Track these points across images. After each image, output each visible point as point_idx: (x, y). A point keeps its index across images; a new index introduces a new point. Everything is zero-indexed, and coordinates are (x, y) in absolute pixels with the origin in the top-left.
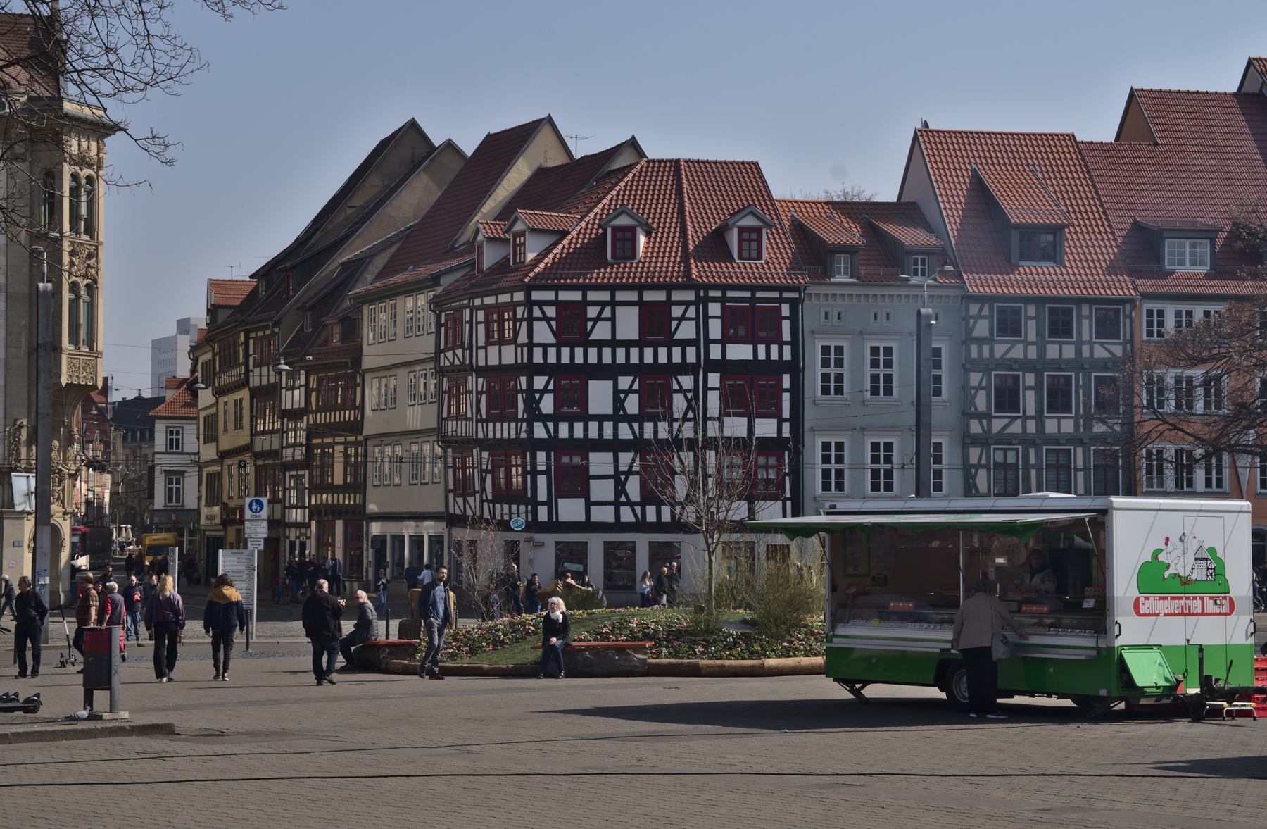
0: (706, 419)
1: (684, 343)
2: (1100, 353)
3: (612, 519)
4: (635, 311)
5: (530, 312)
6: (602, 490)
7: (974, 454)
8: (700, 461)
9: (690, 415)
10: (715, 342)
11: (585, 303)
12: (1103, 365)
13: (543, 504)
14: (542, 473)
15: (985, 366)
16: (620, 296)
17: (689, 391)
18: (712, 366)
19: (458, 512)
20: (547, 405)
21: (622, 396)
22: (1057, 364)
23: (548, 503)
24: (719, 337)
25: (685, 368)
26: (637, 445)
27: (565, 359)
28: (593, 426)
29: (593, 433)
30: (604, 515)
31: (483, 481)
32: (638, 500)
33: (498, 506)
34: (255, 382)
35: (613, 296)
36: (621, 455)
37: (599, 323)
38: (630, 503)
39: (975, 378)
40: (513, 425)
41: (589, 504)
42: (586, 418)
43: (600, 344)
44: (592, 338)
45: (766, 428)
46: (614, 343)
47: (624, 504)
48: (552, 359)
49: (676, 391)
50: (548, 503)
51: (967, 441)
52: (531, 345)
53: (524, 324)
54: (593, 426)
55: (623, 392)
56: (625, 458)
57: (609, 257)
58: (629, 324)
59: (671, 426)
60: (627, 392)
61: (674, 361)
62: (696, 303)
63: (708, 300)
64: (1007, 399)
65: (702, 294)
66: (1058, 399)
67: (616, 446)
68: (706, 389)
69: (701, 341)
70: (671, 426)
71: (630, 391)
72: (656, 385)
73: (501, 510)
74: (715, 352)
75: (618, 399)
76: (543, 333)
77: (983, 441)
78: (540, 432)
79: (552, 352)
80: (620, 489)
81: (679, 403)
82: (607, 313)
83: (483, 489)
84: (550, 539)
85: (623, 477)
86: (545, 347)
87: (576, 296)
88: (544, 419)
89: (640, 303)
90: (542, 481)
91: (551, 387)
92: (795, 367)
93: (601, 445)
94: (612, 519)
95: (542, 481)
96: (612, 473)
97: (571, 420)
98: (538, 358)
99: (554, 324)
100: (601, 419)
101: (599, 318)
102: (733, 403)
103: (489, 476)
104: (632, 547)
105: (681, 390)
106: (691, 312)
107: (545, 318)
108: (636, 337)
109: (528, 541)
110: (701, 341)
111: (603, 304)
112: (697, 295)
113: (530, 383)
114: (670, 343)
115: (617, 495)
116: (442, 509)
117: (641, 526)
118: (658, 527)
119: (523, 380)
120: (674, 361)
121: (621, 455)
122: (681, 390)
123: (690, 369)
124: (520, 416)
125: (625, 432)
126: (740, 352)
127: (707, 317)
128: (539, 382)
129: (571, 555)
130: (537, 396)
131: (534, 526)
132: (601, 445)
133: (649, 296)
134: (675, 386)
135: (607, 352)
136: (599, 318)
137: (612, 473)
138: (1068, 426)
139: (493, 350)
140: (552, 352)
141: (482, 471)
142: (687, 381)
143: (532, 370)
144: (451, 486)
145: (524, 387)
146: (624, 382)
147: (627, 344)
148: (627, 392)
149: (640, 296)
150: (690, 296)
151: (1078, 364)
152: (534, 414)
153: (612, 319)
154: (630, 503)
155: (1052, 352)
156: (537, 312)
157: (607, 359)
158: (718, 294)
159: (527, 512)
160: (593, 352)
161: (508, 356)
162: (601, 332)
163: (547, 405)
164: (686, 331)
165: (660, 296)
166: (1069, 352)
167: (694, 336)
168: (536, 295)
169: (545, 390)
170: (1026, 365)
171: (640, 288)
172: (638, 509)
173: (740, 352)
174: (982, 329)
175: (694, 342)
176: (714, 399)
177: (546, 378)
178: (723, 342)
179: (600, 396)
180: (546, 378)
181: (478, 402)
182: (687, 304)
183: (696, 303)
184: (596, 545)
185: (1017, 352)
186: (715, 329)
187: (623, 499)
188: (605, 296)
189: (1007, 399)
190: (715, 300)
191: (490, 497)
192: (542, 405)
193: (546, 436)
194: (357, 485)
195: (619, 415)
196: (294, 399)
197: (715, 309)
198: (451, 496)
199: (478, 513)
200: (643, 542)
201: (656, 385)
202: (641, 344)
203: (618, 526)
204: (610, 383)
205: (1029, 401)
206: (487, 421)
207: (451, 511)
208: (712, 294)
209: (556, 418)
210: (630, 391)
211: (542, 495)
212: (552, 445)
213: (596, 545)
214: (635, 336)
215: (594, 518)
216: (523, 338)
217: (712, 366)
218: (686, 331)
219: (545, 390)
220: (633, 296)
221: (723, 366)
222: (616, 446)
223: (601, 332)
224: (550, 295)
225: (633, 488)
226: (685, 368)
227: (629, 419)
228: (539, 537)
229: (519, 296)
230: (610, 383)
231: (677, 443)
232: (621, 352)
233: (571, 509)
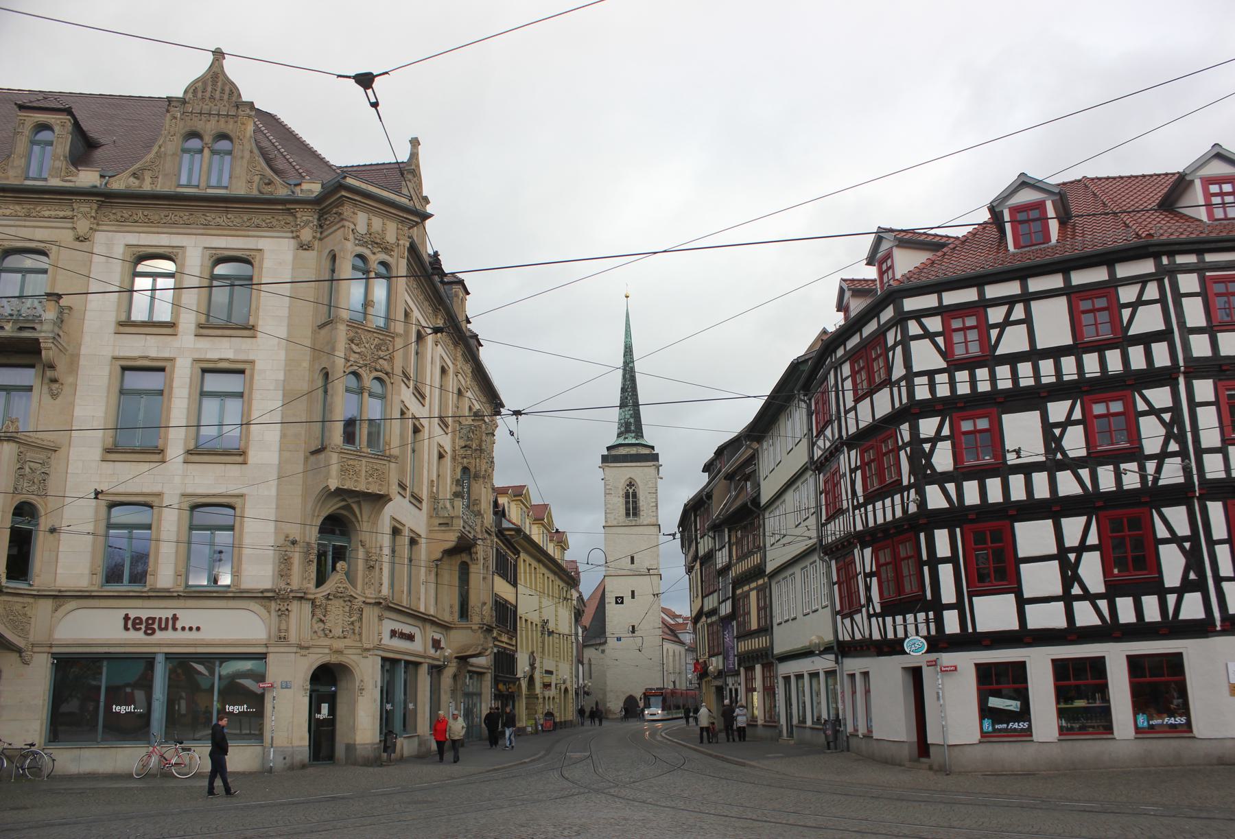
0: (1200, 452)
1: (1147, 340)
3: (1062, 623)
4: (1061, 303)
5: (905, 331)
6: (1041, 579)
8: (1200, 523)
9: (1173, 447)
10: (1198, 331)
11: (984, 304)
13: (950, 607)
14: (945, 560)
16: (1035, 285)
17: (1165, 410)
18: (1198, 369)
19: (847, 638)
20: (943, 459)
21: (1057, 431)
23: (959, 606)
24: (1202, 322)
25: (1154, 377)
27: (963, 389)
28: (1017, 482)
29: (1018, 492)
30: (1048, 617)
31: (868, 588)
32: (1101, 589)
33: (889, 620)
34: (701, 553)
35: (1024, 287)
36: (1065, 522)
37: (1008, 329)
38: (1087, 596)
40: (897, 498)
41: (1022, 602)
42: (1003, 471)
43: (1013, 360)
44: (999, 352)
46: (1034, 355)
47: (1078, 598)
48: (943, 391)
49: (1144, 414)
50: (959, 606)
52: (910, 376)
53: (899, 349)
54: (1017, 482)
55: (1057, 425)
56: (1073, 527)
57: (1011, 247)
58: (1053, 323)
59: (1142, 468)
60: (1064, 425)
61: (1134, 366)
62: (1157, 277)
63: (1173, 272)
65: (1165, 260)
67: (1055, 509)
68: (1193, 405)
70: (1142, 468)
71: (1069, 422)
73: (893, 626)
74: (1200, 346)
75: (1051, 435)
76: (925, 356)
78: (935, 499)
79: (942, 378)
80: (1070, 575)
81: (1152, 434)
82: (1019, 312)
83: (869, 599)
84: (966, 661)
85: (1072, 556)
86: (931, 374)
87: (970, 295)
88: (941, 479)
89: (1068, 291)
90: (946, 572)
91: (946, 431)
93: (1032, 510)
94: (1062, 623)
95: (946, 572)
96: (1054, 551)
97: (981, 474)
98: (922, 393)
99: (940, 340)
100: (1027, 470)
101: (1007, 322)
103: (875, 580)
104: (1098, 666)
105: (1153, 411)
106: (1152, 291)
107: (927, 335)
108: (1068, 340)
109: (933, 664)
111: (1010, 301)
112: (1158, 264)
113: (914, 430)
114: (1123, 341)
115: (1067, 582)
116: (829, 637)
117: (1111, 631)
119: (905, 427)
120: (1134, 366)
121: (1065, 522)
122: (1153, 411)
123: (1165, 377)
124: (905, 482)
125: (1068, 485)
127: (1178, 296)
128: (928, 426)
129: (1002, 682)
130: (927, 447)
131: (939, 643)
132: (1032, 510)
133: (1080, 278)
134: (1141, 406)
135: (1025, 369)
136: (1007, 322)
137: (1054, 551)
139: (864, 406)
140: (942, 378)
141: (866, 575)
142: (1160, 397)
143: (912, 411)
144: (838, 608)
145: (907, 438)
146: (1058, 410)
147: (1056, 353)
148: (1064, 425)
149: (1067, 280)
150: (1148, 267)
152: (925, 474)
153: (1028, 321)
154: (1087, 596)
156: (914, 328)
157: (1027, 381)
158: (1192, 259)
159: (927, 621)
160: (1003, 371)
161: (883, 403)
162: (1014, 341)
163: (943, 459)
164: (1148, 320)
165: (1099, 275)
167: (1162, 327)
168: (910, 304)
169: (938, 438)
171: (1065, 267)
172: (1103, 604)
175: (1164, 335)
176: (1208, 418)
177: (937, 420)
178: (1212, 330)
179: (1022, 433)
180: (937, 420)
181: (853, 483)
182: (1143, 280)
183: (1157, 277)
184: (1039, 665)
186: (1194, 313)
187: (1076, 590)
188: (1013, 288)
190: (1187, 269)
191: (878, 610)
192: (935, 460)
193: (945, 505)
194: (766, 630)
195: (1055, 462)
196: (721, 558)
197: (1188, 282)
198: (839, 617)
199: (867, 635)
200: (1116, 656)
202: (1077, 349)
203: (1072, 634)
204: (1036, 415)
206: (865, 505)
207: (841, 638)
208: (1181, 259)
209: (959, 475)
210: (1069, 422)
211: (948, 595)
212: (954, 516)
213: (1039, 665)
214: (1065, 338)
215: (1032, 624)
216: (898, 371)
217: (1198, 369)
219: (938, 438)
220: (1056, 281)
222: (1055, 509)
224: (930, 301)
225: (1091, 570)
226: (1154, 377)
227: (1073, 465)
228: (947, 658)
229: (888, 314)
230: (1037, 414)
232: (1047, 366)
233: (995, 612)
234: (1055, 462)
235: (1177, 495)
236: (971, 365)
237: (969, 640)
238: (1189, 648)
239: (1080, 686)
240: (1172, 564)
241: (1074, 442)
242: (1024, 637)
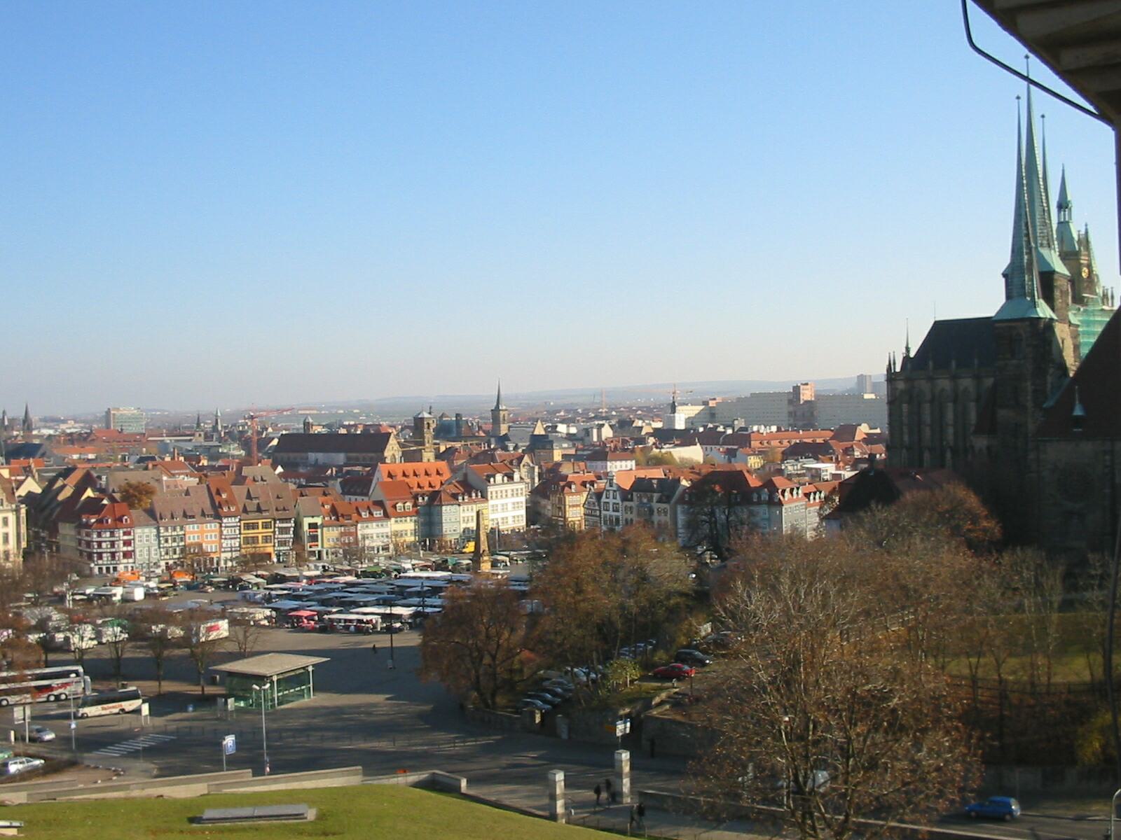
6: (105, 559)
20: (96, 547)
45: (130, 549)
64: (167, 541)
66: (174, 540)
67: (107, 552)
76: (95, 536)
78: (95, 551)
92: (134, 539)
110: (119, 537)
151: (178, 535)
152: (94, 548)
173: (126, 538)
179: (104, 545)
184: (104, 568)
189: (167, 541)
205: (170, 541)
212: (96, 553)
213: (104, 568)
218: (117, 535)
222: (107, 552)
223: (104, 536)
225: (110, 558)
231: (116, 552)
233: (100, 562)
234: (107, 548)
237: (98, 565)
239: (108, 569)
240: (117, 558)
242: (103, 564)
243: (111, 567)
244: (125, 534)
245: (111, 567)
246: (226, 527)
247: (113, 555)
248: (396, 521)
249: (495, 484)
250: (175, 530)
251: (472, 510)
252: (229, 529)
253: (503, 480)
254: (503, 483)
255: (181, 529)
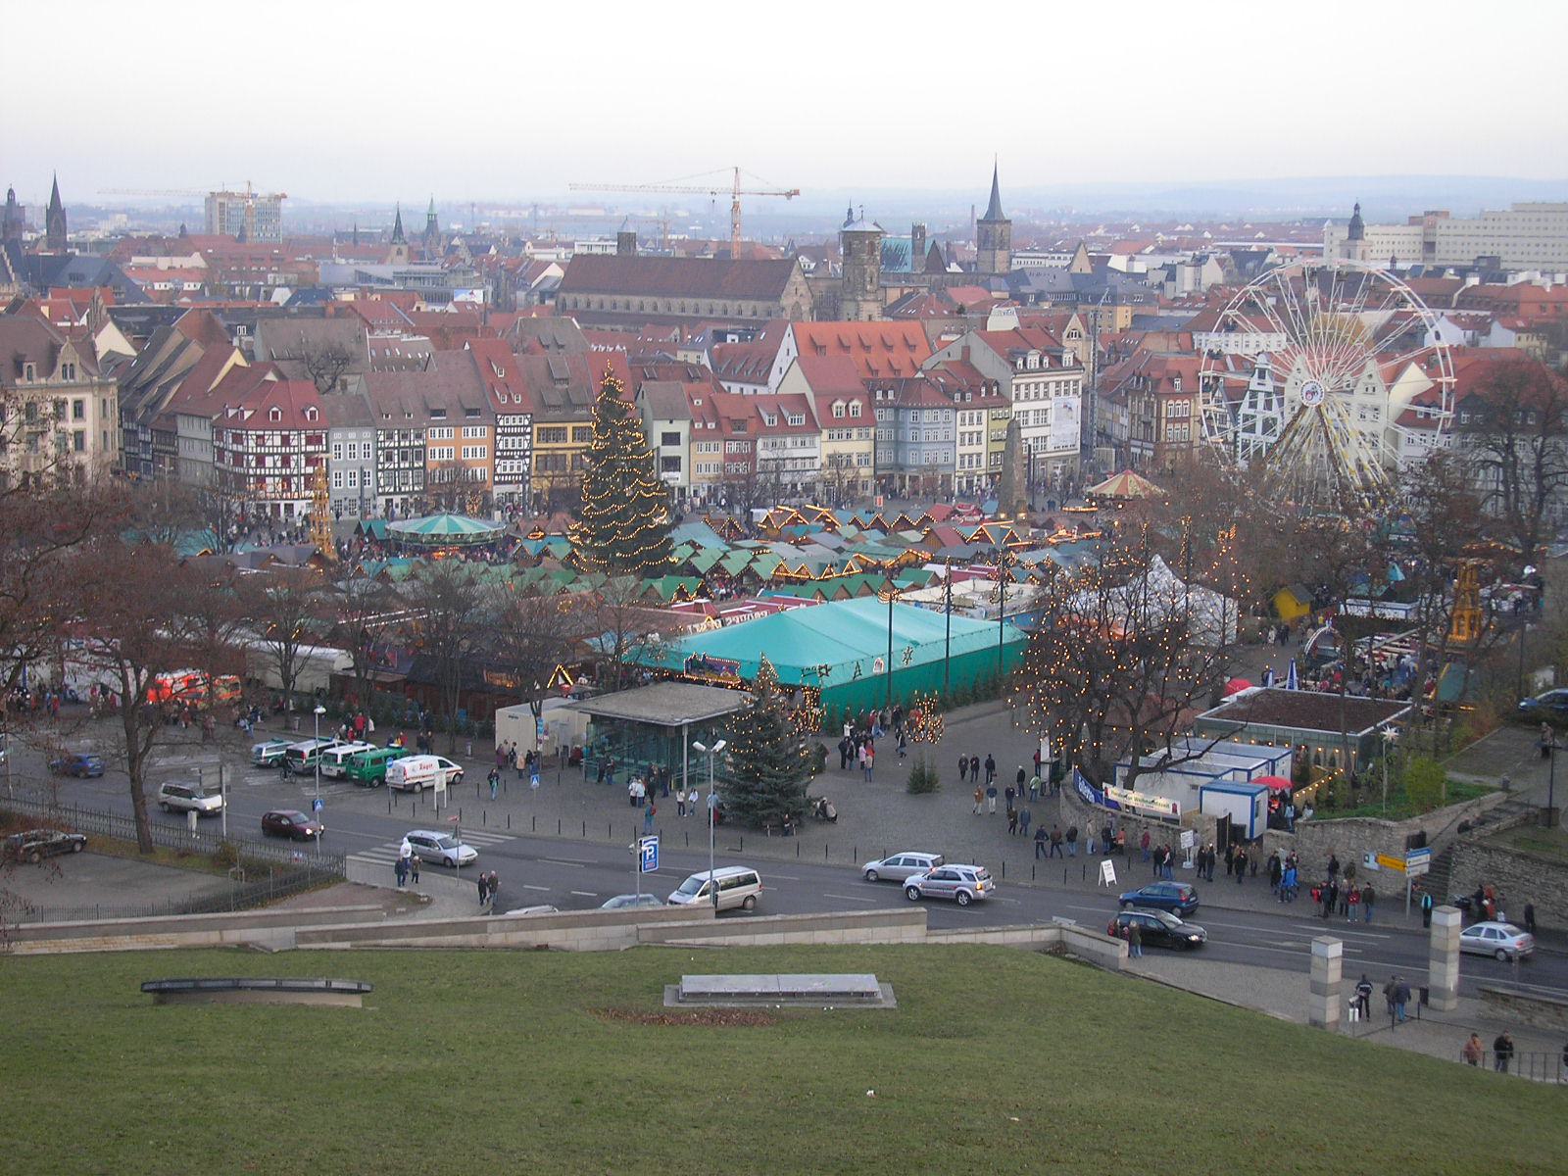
2: (416, 443)
6: (270, 489)
7: (380, 474)
8: (299, 480)
12: (418, 447)
15: (383, 449)
20: (253, 464)
22: (405, 447)
25: (294, 454)
26: (280, 475)
39: (380, 452)
51: (378, 471)
56: (277, 479)
58: (278, 441)
64: (389, 458)
66: (404, 458)
67: (274, 476)
69: (299, 446)
72: (286, 461)
74: (303, 449)
76: (252, 443)
77: (382, 470)
81: (293, 464)
87: (262, 433)
102: (307, 464)
110: (299, 446)
117: (282, 499)
118: (287, 499)
125: (277, 472)
126: (311, 448)
138: (407, 465)
142: (295, 457)
146: (276, 457)
151: (410, 447)
155: (402, 444)
162: (269, 443)
164: (295, 443)
166: (407, 444)
170: (394, 448)
173: (311, 448)
174: (381, 438)
179: (269, 461)
185: (392, 445)
186: (303, 442)
189: (389, 458)
195: (275, 467)
197: (303, 436)
201: (286, 461)
212: (255, 475)
218: (295, 443)
221: (305, 453)
222: (274, 476)
223: (269, 443)
226: (294, 454)
231: (293, 475)
234: (275, 467)
235: (296, 476)
236: (261, 446)
238: (295, 503)
241: (279, 464)
243: (282, 504)
244: (309, 441)
245: (282, 504)
246: (503, 434)
247: (286, 479)
248: (831, 437)
249: (1026, 371)
250: (405, 437)
251: (979, 419)
252: (510, 439)
253: (1041, 362)
254: (1041, 369)
255: (418, 436)
